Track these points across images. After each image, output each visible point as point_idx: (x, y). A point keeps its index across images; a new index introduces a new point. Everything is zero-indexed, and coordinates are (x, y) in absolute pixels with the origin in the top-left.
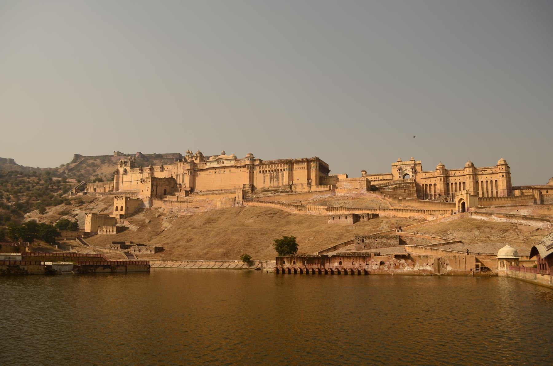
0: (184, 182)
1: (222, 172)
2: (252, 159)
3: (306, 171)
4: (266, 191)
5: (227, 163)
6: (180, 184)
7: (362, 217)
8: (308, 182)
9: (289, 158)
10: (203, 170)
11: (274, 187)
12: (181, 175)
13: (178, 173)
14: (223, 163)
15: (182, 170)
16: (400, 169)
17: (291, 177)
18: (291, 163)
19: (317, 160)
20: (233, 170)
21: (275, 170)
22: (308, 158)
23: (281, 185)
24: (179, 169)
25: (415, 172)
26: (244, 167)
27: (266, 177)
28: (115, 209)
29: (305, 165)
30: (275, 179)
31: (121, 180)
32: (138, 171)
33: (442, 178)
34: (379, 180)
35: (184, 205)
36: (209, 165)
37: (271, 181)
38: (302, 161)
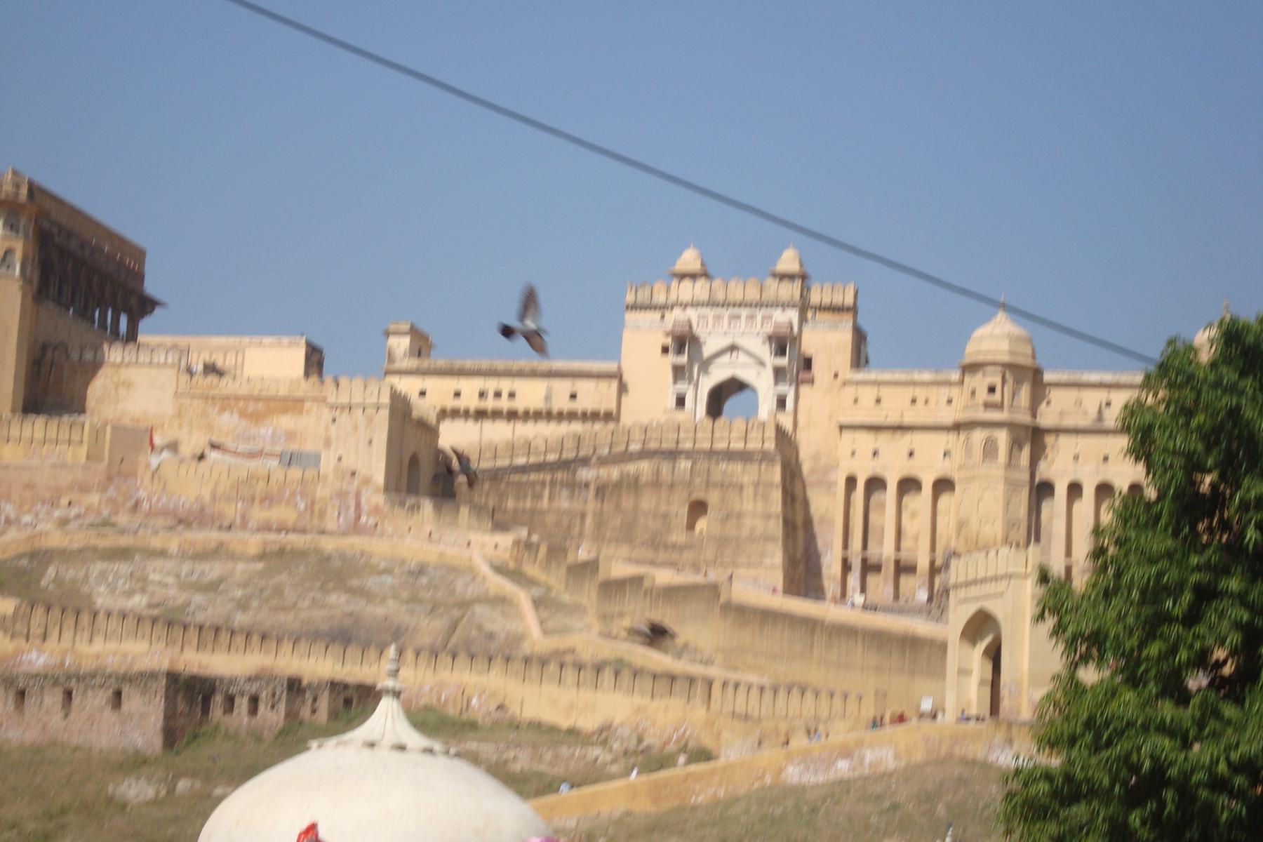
33: (1002, 437)
34: (512, 415)
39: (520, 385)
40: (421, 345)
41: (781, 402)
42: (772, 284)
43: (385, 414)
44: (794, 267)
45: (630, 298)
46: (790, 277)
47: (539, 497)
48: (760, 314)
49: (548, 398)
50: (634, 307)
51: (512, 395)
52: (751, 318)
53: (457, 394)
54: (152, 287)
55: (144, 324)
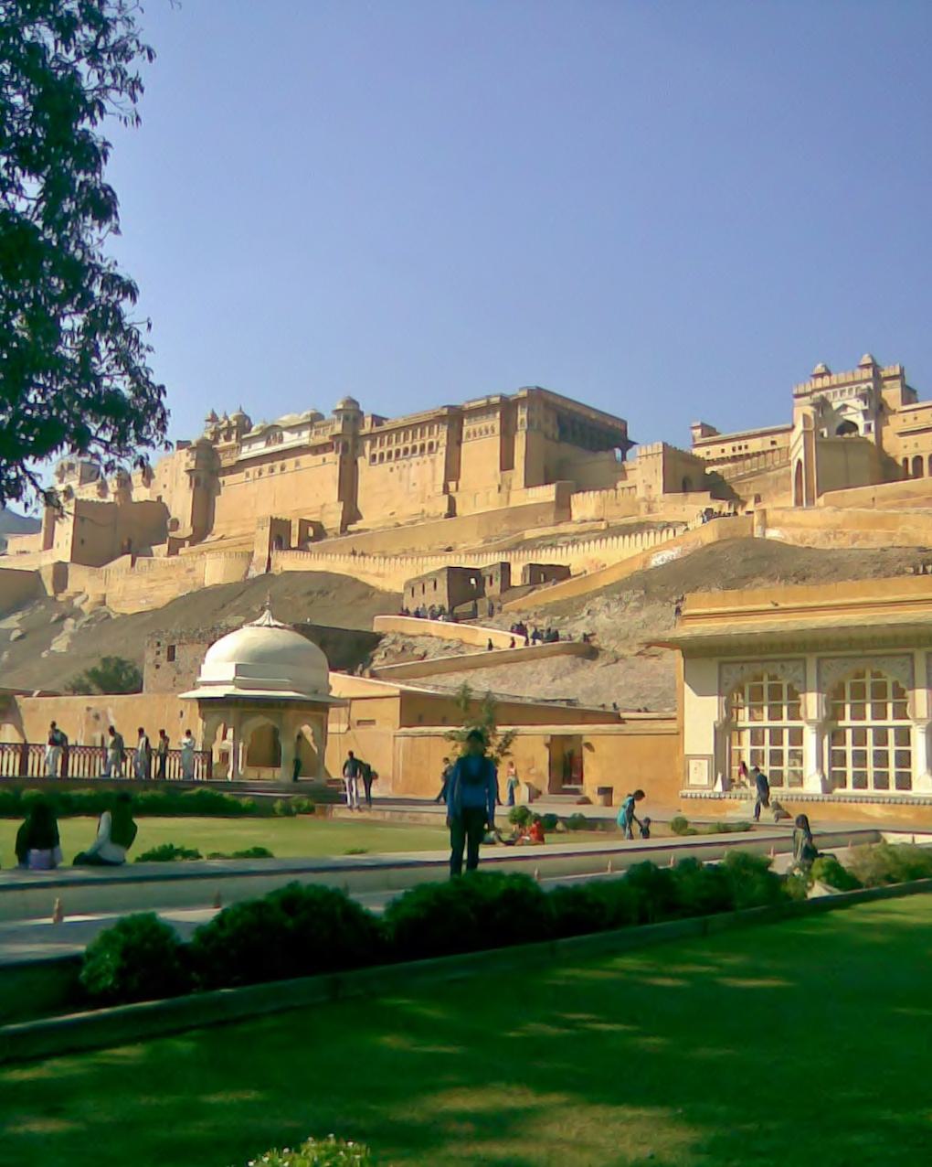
1: (278, 470)
2: (352, 414)
3: (499, 438)
5: (290, 440)
7: (488, 579)
9: (458, 401)
14: (281, 440)
16: (822, 405)
17: (453, 471)
18: (454, 418)
19: (538, 397)
20: (306, 459)
22: (508, 393)
25: (879, 411)
29: (494, 422)
36: (247, 452)
38: (486, 410)
39: (749, 442)
40: (708, 430)
41: (868, 428)
42: (858, 371)
43: (661, 456)
44: (868, 361)
45: (795, 392)
46: (867, 366)
47: (748, 489)
48: (854, 387)
49: (762, 445)
50: (798, 396)
51: (746, 447)
52: (851, 390)
53: (723, 451)
54: (631, 436)
55: (629, 453)
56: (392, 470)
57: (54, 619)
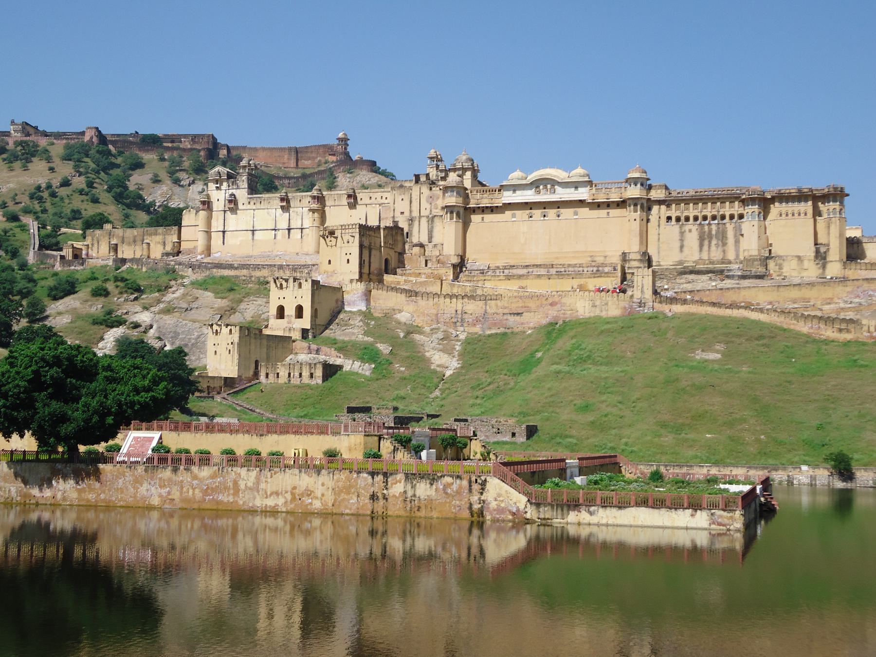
0: (435, 240)
4: (691, 272)
6: (422, 246)
8: (817, 251)
10: (492, 210)
11: (712, 263)
12: (424, 221)
13: (415, 214)
15: (425, 204)
21: (714, 218)
23: (731, 256)
24: (415, 204)
26: (622, 204)
27: (687, 234)
28: (273, 311)
30: (714, 242)
31: (217, 224)
32: (278, 203)
35: (473, 308)
36: (508, 197)
37: (701, 246)
56: (690, 231)
57: (402, 335)
